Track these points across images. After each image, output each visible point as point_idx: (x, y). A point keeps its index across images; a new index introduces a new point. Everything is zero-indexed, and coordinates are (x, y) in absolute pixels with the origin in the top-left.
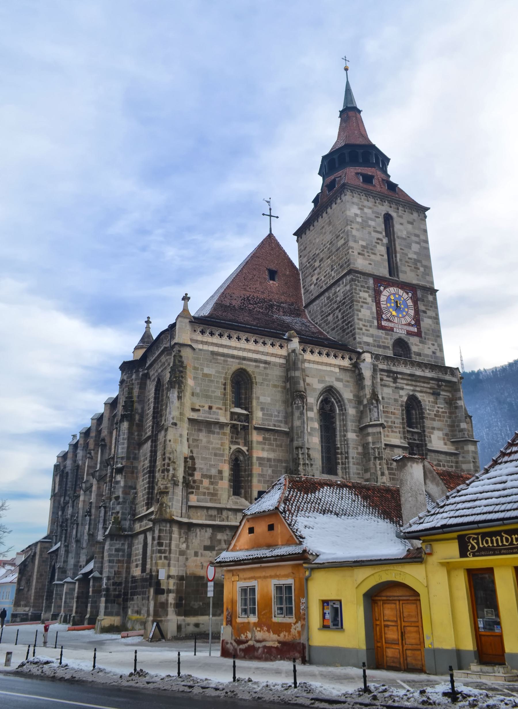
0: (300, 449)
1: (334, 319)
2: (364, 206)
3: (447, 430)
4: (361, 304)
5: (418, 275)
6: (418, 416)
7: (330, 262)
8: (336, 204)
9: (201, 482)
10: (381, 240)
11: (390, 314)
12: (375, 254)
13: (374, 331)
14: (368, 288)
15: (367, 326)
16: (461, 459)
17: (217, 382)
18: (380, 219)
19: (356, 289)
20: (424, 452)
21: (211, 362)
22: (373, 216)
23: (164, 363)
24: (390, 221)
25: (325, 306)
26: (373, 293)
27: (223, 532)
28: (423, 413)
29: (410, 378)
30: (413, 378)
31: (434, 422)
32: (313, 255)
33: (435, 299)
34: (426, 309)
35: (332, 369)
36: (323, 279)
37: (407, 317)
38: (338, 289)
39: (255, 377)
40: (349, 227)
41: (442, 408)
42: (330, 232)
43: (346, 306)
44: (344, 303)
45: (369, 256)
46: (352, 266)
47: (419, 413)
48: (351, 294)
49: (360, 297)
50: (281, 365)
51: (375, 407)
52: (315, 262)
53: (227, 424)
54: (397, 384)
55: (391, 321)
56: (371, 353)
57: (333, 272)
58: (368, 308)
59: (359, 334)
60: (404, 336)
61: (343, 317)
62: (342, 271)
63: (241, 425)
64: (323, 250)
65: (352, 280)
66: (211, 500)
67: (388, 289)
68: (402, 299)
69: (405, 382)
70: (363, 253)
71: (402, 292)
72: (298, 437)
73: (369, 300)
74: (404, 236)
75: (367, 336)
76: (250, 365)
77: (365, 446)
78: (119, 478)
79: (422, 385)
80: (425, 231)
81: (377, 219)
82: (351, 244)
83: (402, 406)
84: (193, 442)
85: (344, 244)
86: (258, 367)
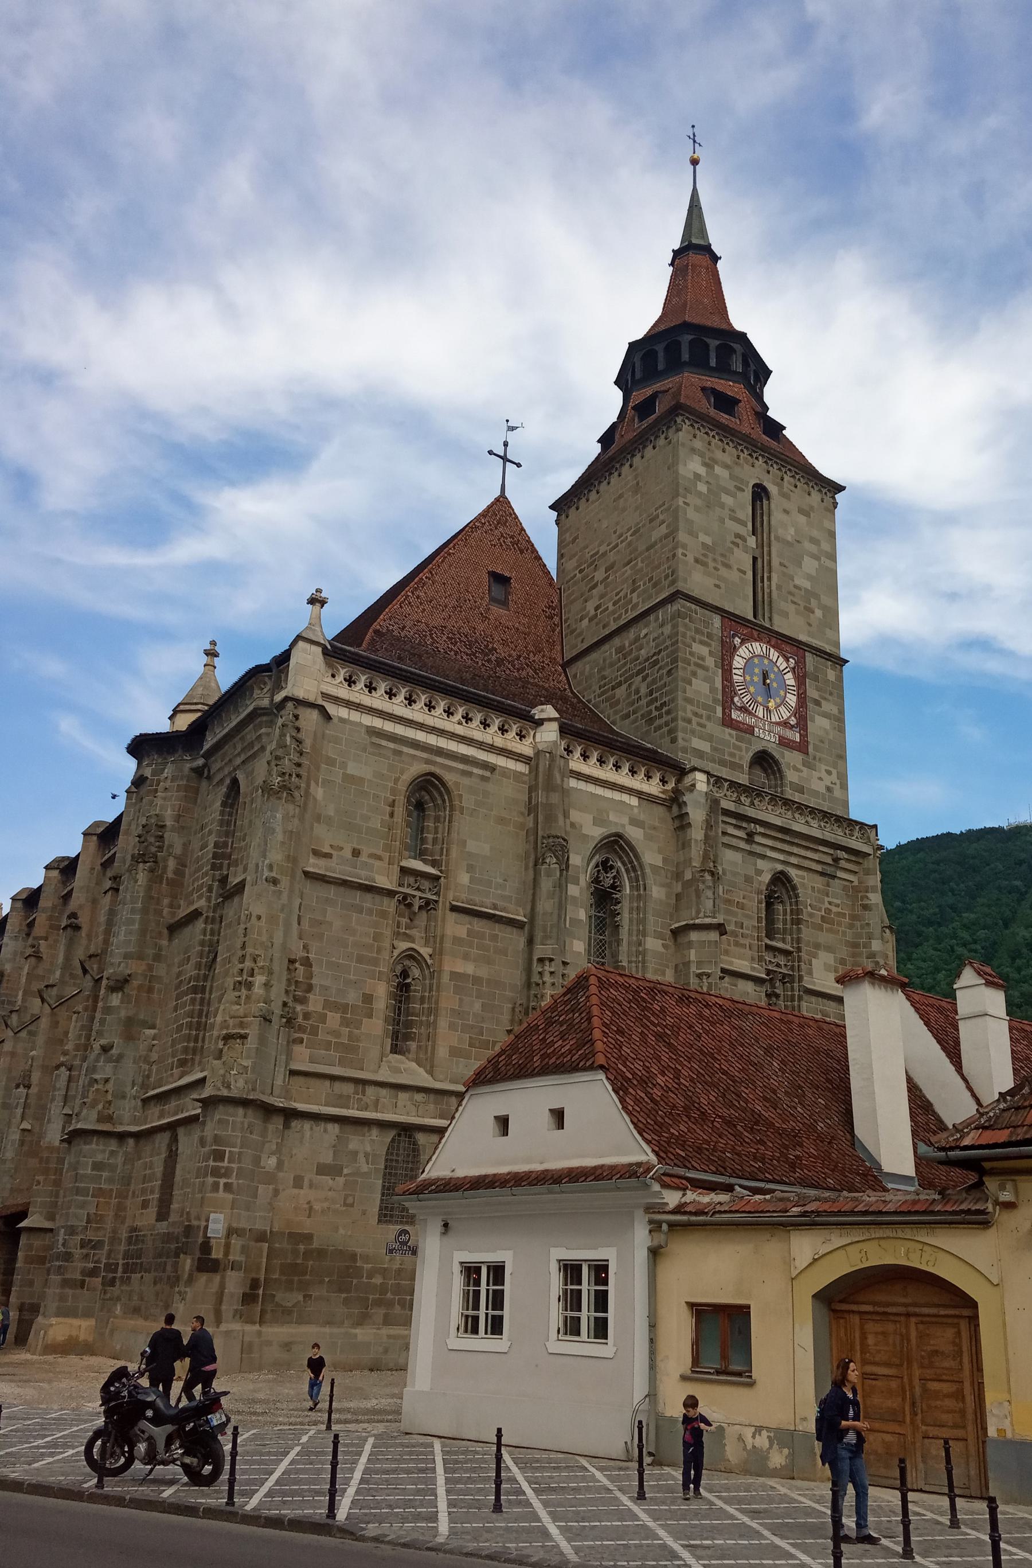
0: (547, 963)
1: (629, 695)
3: (844, 952)
4: (693, 668)
5: (810, 625)
6: (788, 918)
7: (629, 572)
8: (654, 448)
9: (323, 1018)
10: (745, 540)
11: (749, 697)
12: (728, 566)
13: (714, 728)
14: (710, 636)
15: (701, 717)
17: (376, 797)
18: (746, 493)
19: (684, 635)
20: (797, 993)
21: (364, 750)
22: (731, 485)
23: (251, 745)
24: (765, 502)
25: (612, 665)
27: (364, 1135)
28: (799, 912)
29: (780, 836)
30: (788, 838)
31: (820, 933)
32: (592, 556)
33: (840, 678)
34: (820, 696)
35: (625, 798)
36: (611, 608)
37: (782, 709)
38: (644, 632)
39: (461, 796)
40: (680, 501)
41: (837, 906)
42: (637, 508)
43: (660, 668)
44: (656, 662)
45: (716, 569)
46: (680, 586)
47: (792, 914)
48: (672, 645)
49: (692, 654)
50: (517, 775)
51: (709, 887)
52: (595, 569)
53: (390, 893)
54: (754, 846)
55: (750, 713)
56: (708, 773)
57: (635, 595)
58: (706, 680)
61: (651, 693)
62: (657, 594)
63: (421, 898)
64: (617, 545)
65: (679, 614)
66: (342, 1063)
67: (748, 645)
68: (776, 669)
69: (770, 843)
70: (705, 560)
71: (776, 654)
72: (546, 937)
73: (710, 662)
74: (789, 538)
76: (450, 769)
79: (803, 852)
80: (832, 535)
81: (739, 494)
82: (682, 536)
83: (759, 892)
84: (310, 927)
85: (666, 536)
86: (469, 774)
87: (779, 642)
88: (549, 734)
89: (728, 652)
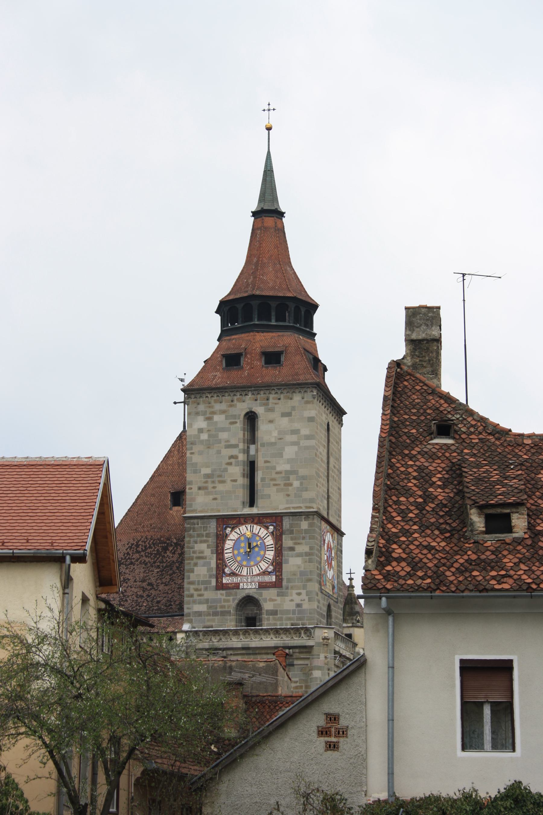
2: (214, 413)
12: (223, 482)
15: (200, 590)
26: (215, 541)
49: (194, 552)
59: (189, 603)
60: (252, 593)
67: (237, 530)
73: (208, 552)
74: (273, 440)
75: (200, 603)
81: (232, 426)
87: (261, 518)
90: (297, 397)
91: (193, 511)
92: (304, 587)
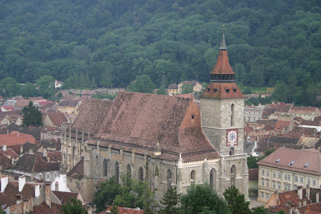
2: (226, 104)
12: (227, 121)
14: (225, 134)
16: (244, 180)
35: (214, 163)
50: (202, 166)
74: (237, 111)
77: (220, 183)
78: (156, 191)
88: (206, 160)
89: (227, 134)
90: (241, 100)
91: (222, 128)
92: (242, 145)
